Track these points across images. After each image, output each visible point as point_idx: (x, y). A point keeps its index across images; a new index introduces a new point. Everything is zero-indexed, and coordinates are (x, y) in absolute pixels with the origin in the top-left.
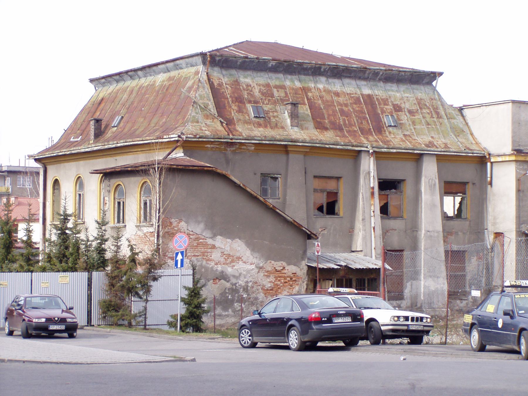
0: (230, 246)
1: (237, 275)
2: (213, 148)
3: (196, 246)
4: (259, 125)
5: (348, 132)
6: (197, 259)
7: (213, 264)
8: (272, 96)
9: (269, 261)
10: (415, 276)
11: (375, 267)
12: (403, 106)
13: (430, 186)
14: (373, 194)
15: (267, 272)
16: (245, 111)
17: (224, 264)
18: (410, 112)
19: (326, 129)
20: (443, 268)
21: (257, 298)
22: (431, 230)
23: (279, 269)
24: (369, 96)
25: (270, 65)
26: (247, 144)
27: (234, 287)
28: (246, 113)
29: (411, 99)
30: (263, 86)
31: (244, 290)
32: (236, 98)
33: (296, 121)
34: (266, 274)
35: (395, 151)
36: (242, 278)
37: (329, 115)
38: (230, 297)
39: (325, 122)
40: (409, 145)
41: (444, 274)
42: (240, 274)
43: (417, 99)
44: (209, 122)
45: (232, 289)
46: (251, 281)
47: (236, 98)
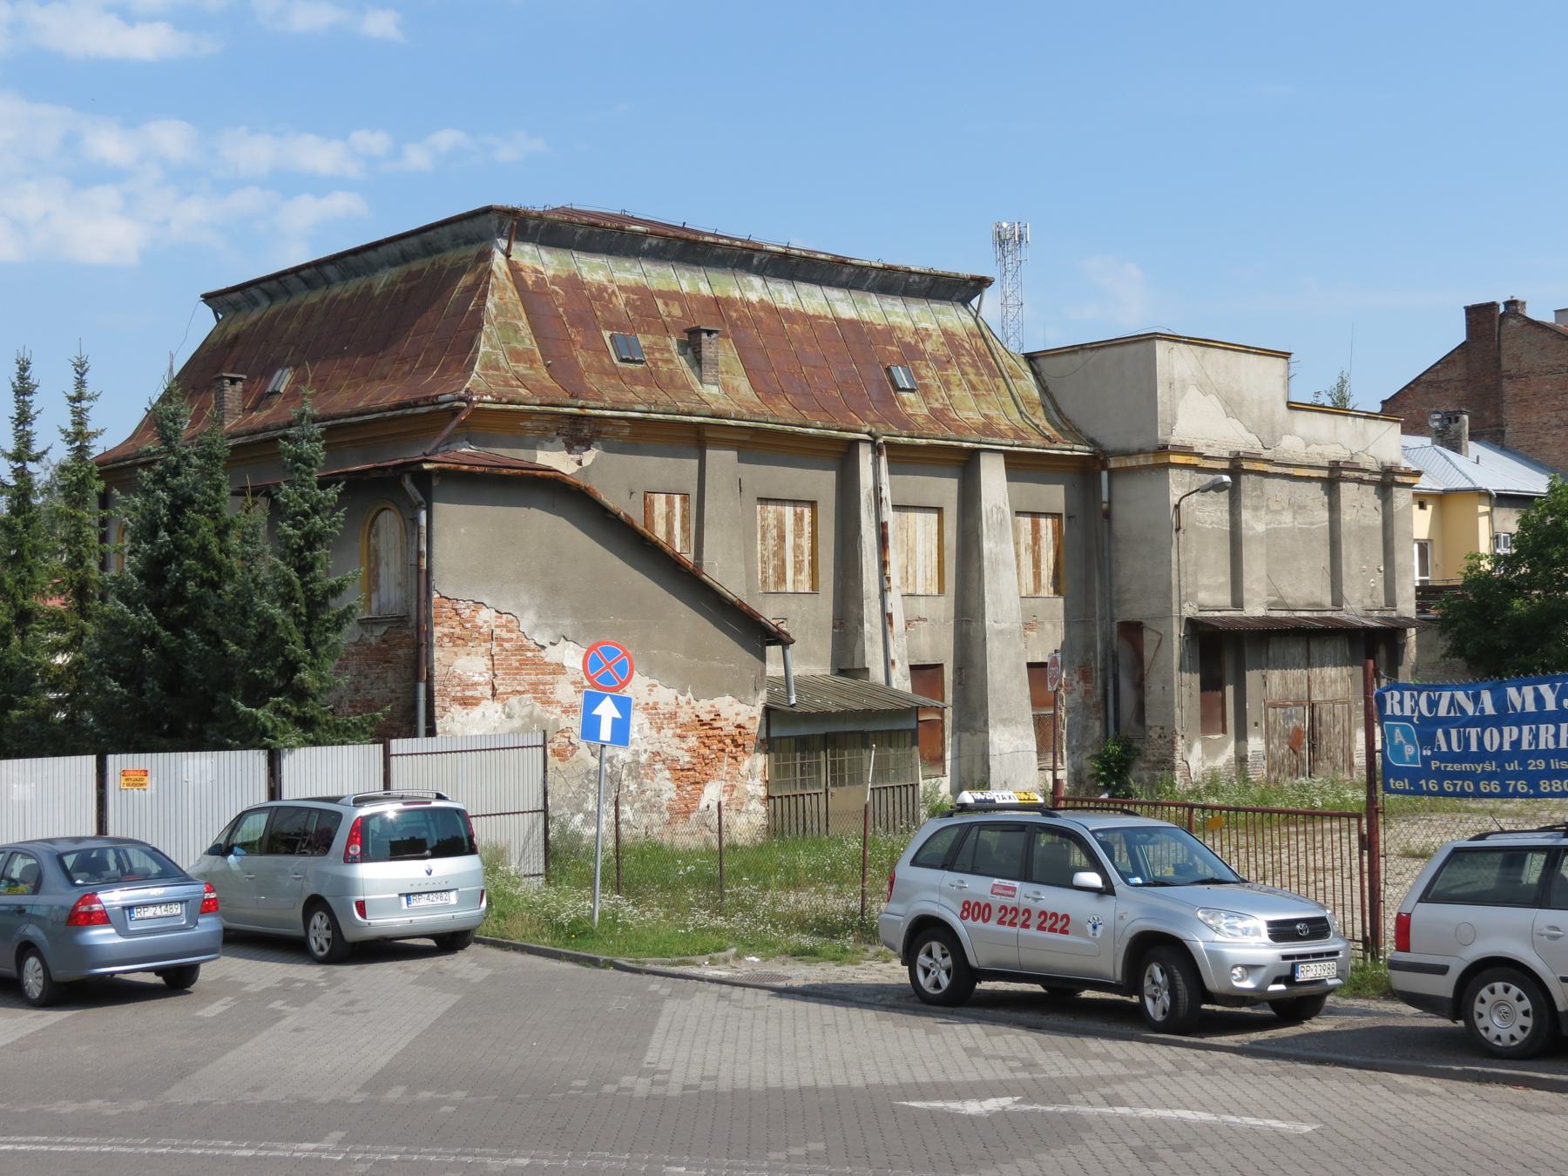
4: (635, 379)
15: (682, 725)
18: (935, 360)
23: (706, 717)
26: (615, 422)
35: (924, 441)
41: (1028, 713)
44: (522, 368)
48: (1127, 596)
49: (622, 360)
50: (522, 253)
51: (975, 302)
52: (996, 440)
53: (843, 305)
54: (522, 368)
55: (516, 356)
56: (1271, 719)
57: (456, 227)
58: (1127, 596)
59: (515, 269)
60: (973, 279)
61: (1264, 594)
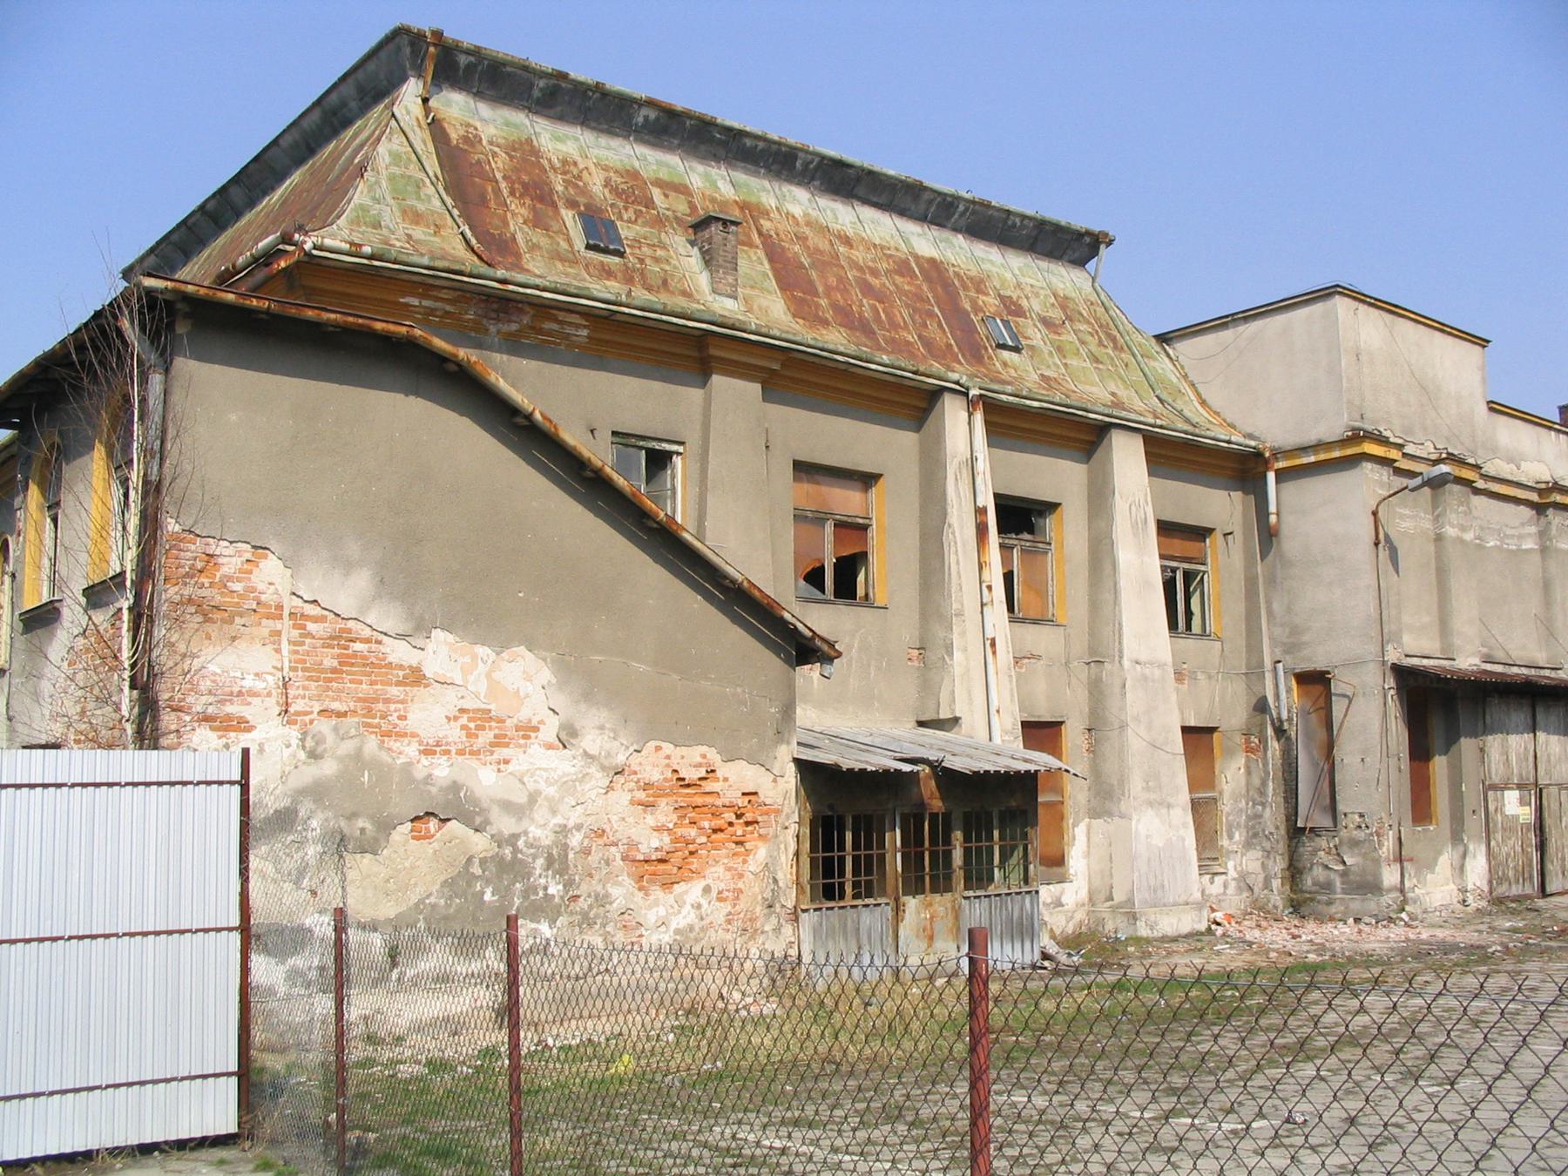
0: (488, 676)
1: (521, 798)
2: (432, 311)
3: (334, 671)
4: (608, 273)
6: (336, 729)
7: (411, 750)
8: (650, 203)
9: (652, 744)
10: (1105, 800)
12: (1024, 303)
13: (1134, 526)
14: (982, 530)
15: (647, 786)
16: (555, 226)
17: (461, 752)
18: (1047, 322)
19: (825, 323)
21: (607, 895)
22: (1143, 658)
23: (691, 775)
25: (640, 120)
26: (561, 316)
27: (508, 851)
28: (560, 232)
29: (1042, 292)
30: (616, 172)
32: (525, 186)
33: (730, 279)
34: (641, 795)
35: (1036, 404)
36: (541, 813)
37: (829, 290)
38: (488, 897)
39: (818, 306)
41: (1184, 797)
42: (533, 798)
44: (418, 233)
45: (499, 861)
46: (579, 827)
47: (525, 186)
48: (1306, 638)
49: (588, 247)
50: (449, 104)
51: (1091, 265)
53: (924, 241)
54: (418, 233)
55: (416, 218)
56: (1491, 808)
57: (360, 75)
58: (1306, 638)
59: (436, 127)
60: (1088, 233)
61: (1477, 642)
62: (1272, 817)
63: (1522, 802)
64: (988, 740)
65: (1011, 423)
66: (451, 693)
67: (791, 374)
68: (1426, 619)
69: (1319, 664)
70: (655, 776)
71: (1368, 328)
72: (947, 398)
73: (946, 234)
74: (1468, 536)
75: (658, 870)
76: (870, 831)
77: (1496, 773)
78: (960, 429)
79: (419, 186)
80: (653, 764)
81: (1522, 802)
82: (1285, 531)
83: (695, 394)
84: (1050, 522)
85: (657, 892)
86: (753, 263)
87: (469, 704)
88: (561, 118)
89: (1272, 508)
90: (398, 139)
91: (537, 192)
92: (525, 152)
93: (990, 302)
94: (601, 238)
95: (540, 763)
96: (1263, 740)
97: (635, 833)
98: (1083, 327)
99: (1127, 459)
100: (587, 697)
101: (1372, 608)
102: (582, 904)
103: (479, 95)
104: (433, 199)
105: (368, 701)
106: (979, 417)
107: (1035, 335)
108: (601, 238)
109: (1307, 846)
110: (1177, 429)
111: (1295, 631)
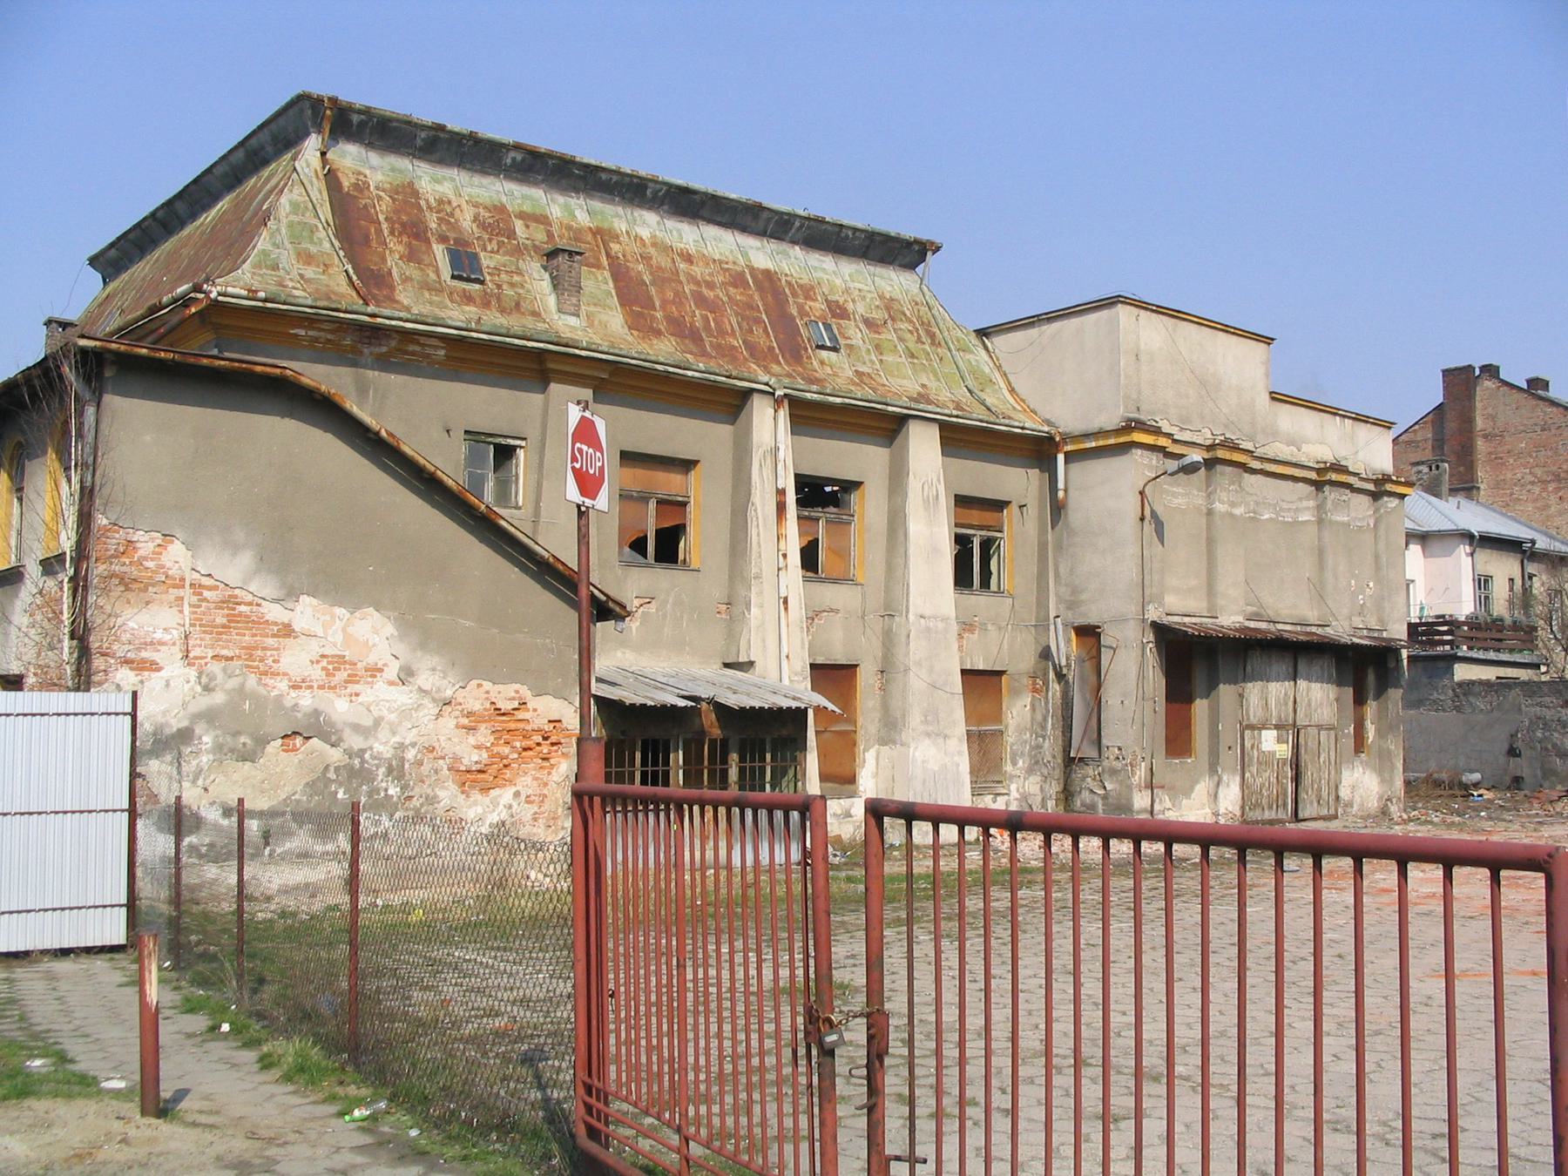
0: (344, 630)
1: (368, 722)
2: (316, 340)
3: (224, 626)
4: (468, 299)
5: (718, 347)
6: (224, 670)
7: (283, 685)
8: (511, 234)
9: (474, 682)
10: (891, 729)
11: (794, 704)
12: (850, 307)
13: (926, 501)
14: (781, 508)
15: (470, 714)
16: (426, 259)
17: (321, 687)
18: (869, 323)
19: (658, 333)
20: (960, 714)
21: (436, 796)
22: (927, 613)
23: (506, 706)
24: (767, 273)
25: (509, 161)
26: (423, 340)
27: (357, 761)
28: (430, 265)
29: (869, 296)
30: (485, 208)
31: (390, 770)
32: (403, 225)
33: (574, 300)
34: (465, 721)
35: (838, 400)
36: (383, 734)
37: (664, 303)
38: (340, 795)
39: (653, 318)
40: (870, 394)
41: (961, 728)
42: (378, 722)
43: (881, 297)
44: (310, 272)
46: (414, 745)
47: (403, 225)
48: (1084, 597)
49: (453, 277)
50: (343, 155)
51: (920, 269)
52: (930, 408)
53: (760, 254)
54: (310, 272)
55: (307, 258)
56: (1248, 744)
57: (273, 126)
58: (1084, 597)
60: (916, 241)
61: (1242, 603)
62: (1051, 747)
63: (1279, 740)
64: (779, 679)
65: (810, 416)
66: (314, 643)
67: (616, 381)
68: (1193, 582)
69: (1092, 619)
70: (477, 706)
71: (1150, 332)
72: (757, 401)
73: (784, 246)
74: (1238, 511)
75: (476, 779)
76: (656, 752)
77: (1254, 712)
78: (768, 425)
79: (312, 230)
80: (475, 697)
81: (1279, 740)
82: (1072, 503)
83: (537, 398)
84: (854, 497)
85: (476, 795)
86: (597, 283)
87: (329, 651)
88: (441, 162)
89: (1061, 485)
90: (298, 190)
91: (414, 231)
92: (407, 194)
93: (818, 307)
94: (465, 265)
95: (384, 697)
96: (1046, 683)
97: (458, 750)
98: (904, 326)
99: (923, 445)
100: (423, 646)
101: (1134, 574)
102: (416, 803)
103: (370, 145)
104: (325, 242)
105: (250, 649)
106: (783, 414)
107: (856, 334)
108: (465, 265)
109: (1079, 772)
110: (976, 416)
111: (1075, 591)
